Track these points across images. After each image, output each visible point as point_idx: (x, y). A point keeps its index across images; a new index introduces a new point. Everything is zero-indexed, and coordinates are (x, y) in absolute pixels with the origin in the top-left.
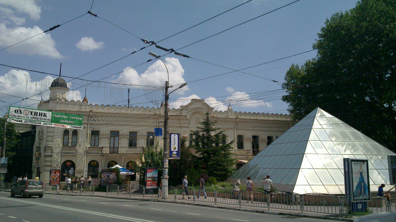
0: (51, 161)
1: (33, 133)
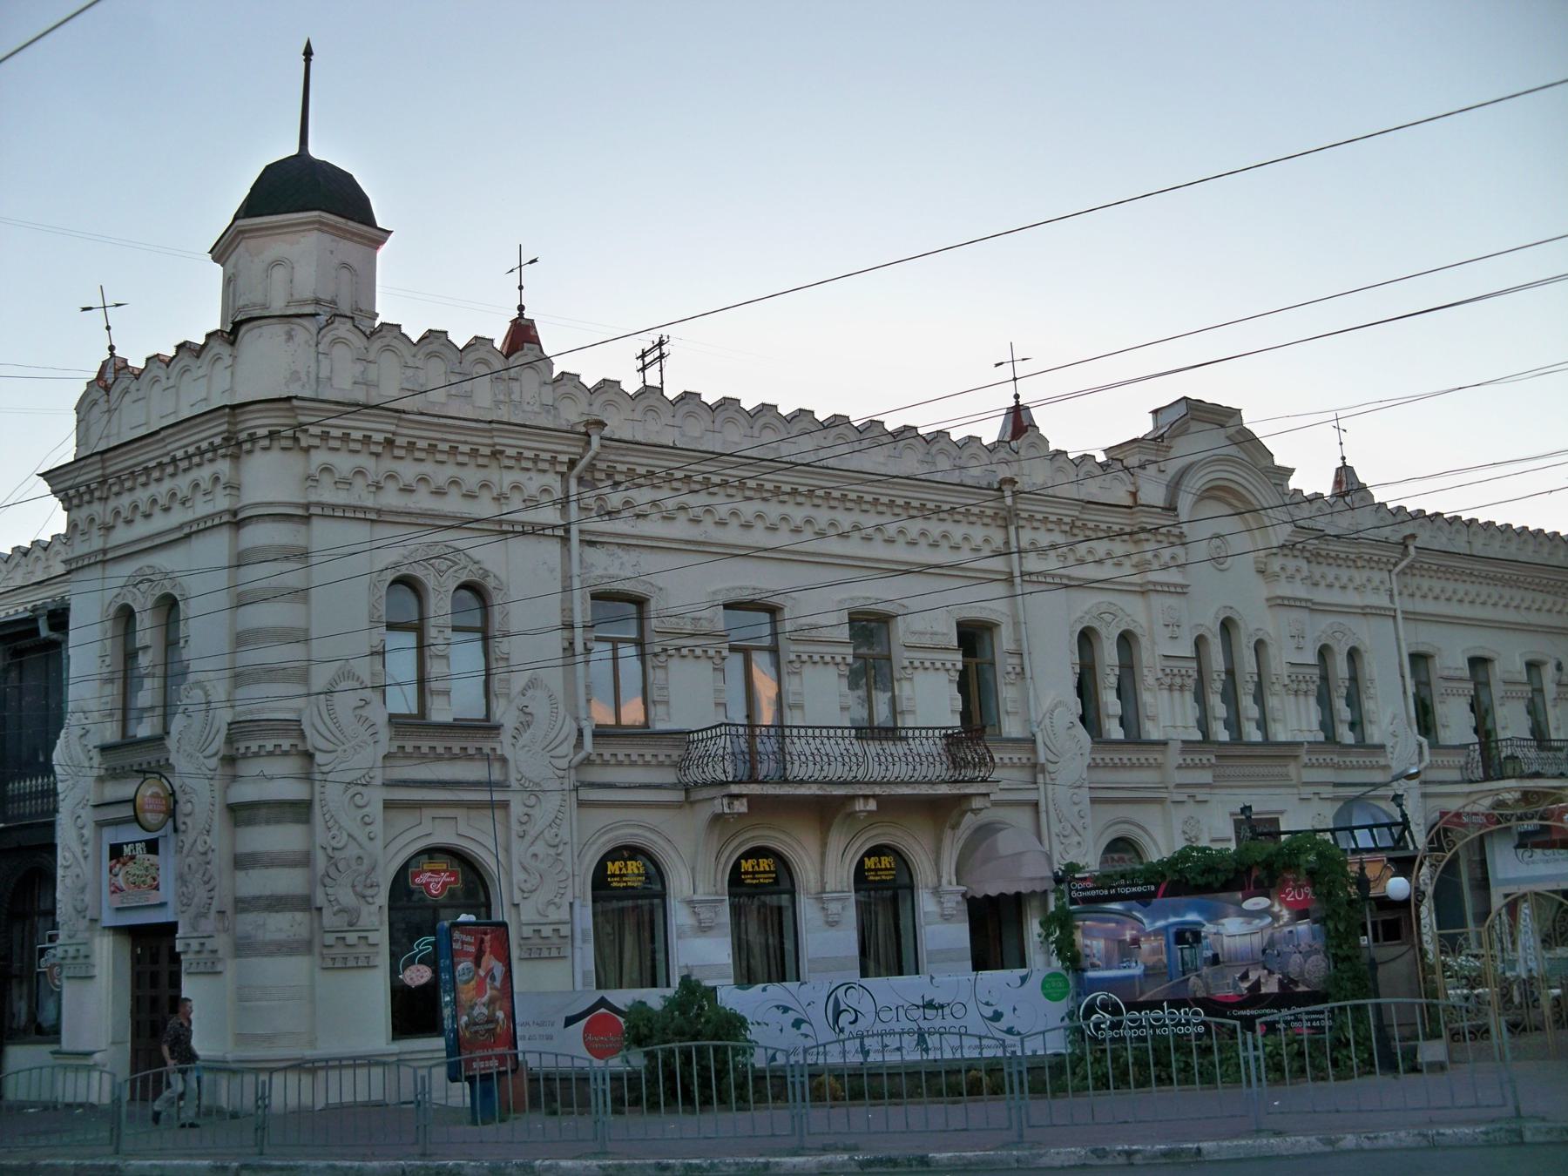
0: (304, 860)
1: (44, 632)
